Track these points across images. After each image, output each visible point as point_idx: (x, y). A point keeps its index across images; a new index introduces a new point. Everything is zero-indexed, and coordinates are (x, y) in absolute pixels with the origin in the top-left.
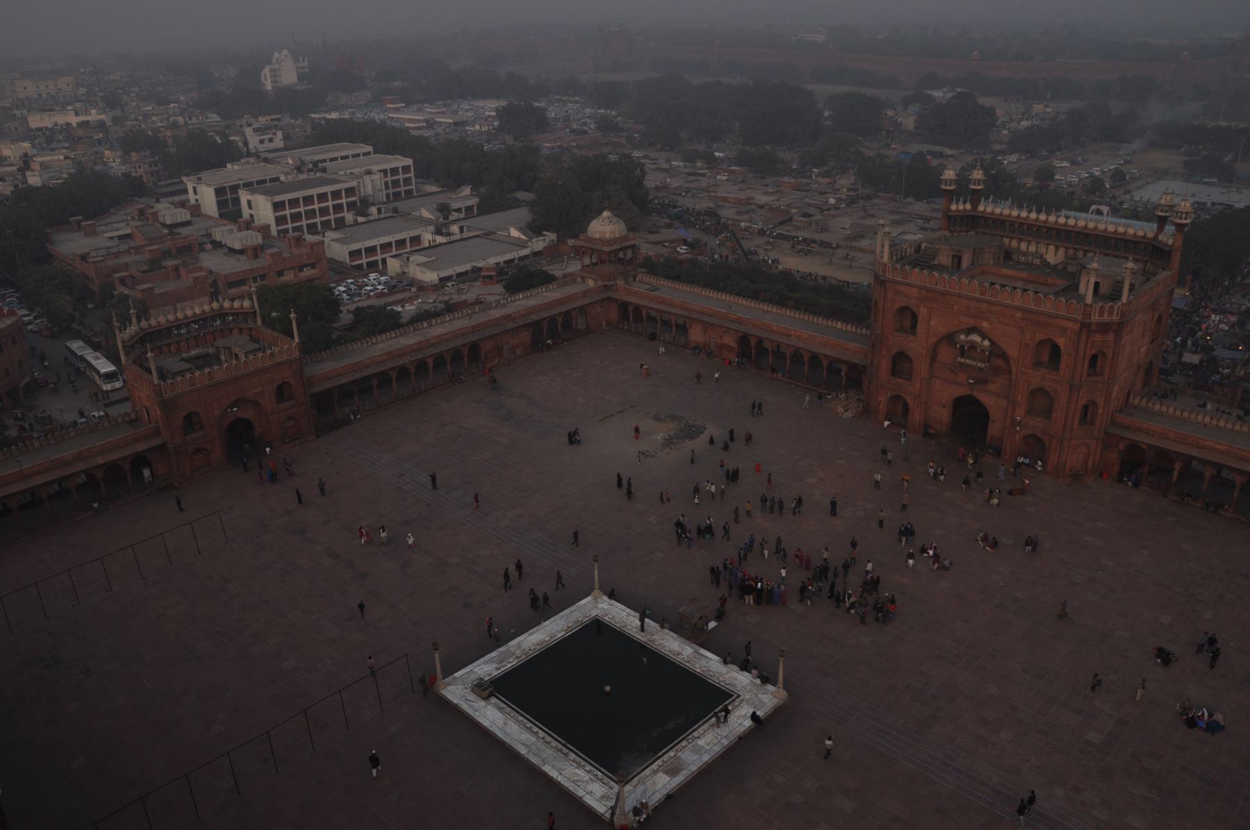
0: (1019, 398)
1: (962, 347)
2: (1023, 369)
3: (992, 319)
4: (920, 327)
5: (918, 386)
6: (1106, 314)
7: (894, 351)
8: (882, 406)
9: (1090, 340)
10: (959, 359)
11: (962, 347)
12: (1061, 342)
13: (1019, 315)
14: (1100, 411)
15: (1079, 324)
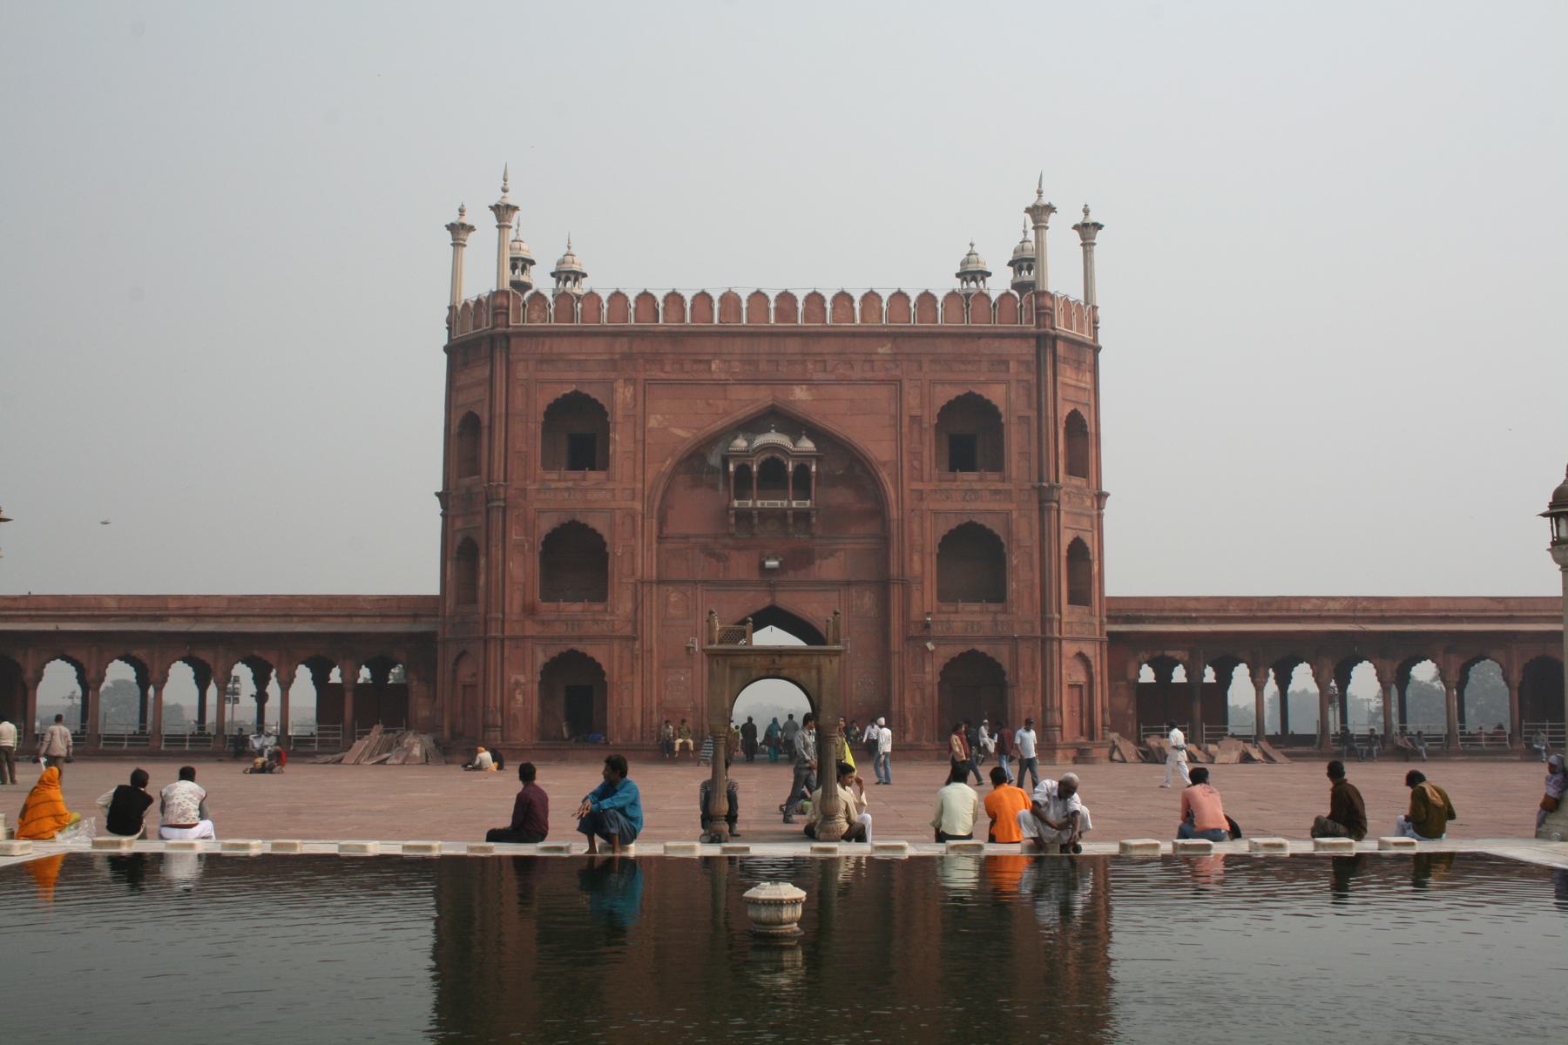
0: (917, 566)
1: (743, 470)
2: (918, 486)
3: (821, 376)
4: (620, 441)
5: (629, 606)
6: (1075, 325)
7: (546, 525)
8: (519, 697)
9: (1059, 378)
10: (736, 503)
11: (743, 470)
12: (995, 394)
13: (885, 349)
14: (1096, 568)
15: (1033, 342)
